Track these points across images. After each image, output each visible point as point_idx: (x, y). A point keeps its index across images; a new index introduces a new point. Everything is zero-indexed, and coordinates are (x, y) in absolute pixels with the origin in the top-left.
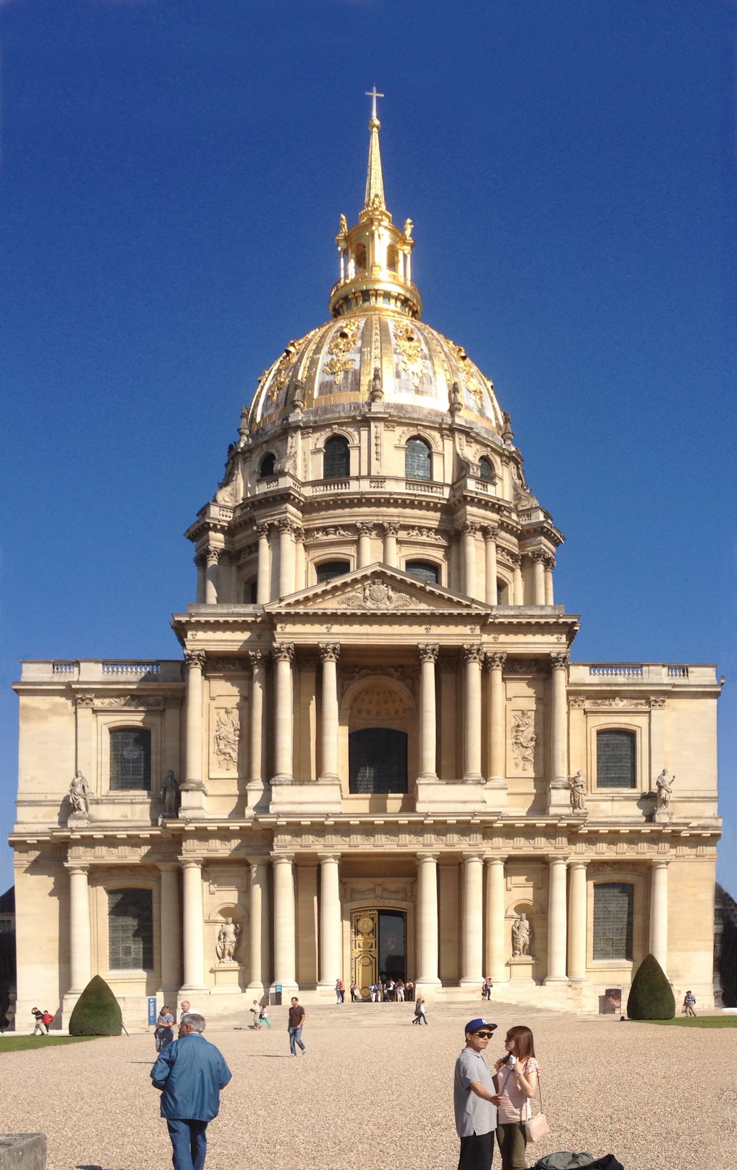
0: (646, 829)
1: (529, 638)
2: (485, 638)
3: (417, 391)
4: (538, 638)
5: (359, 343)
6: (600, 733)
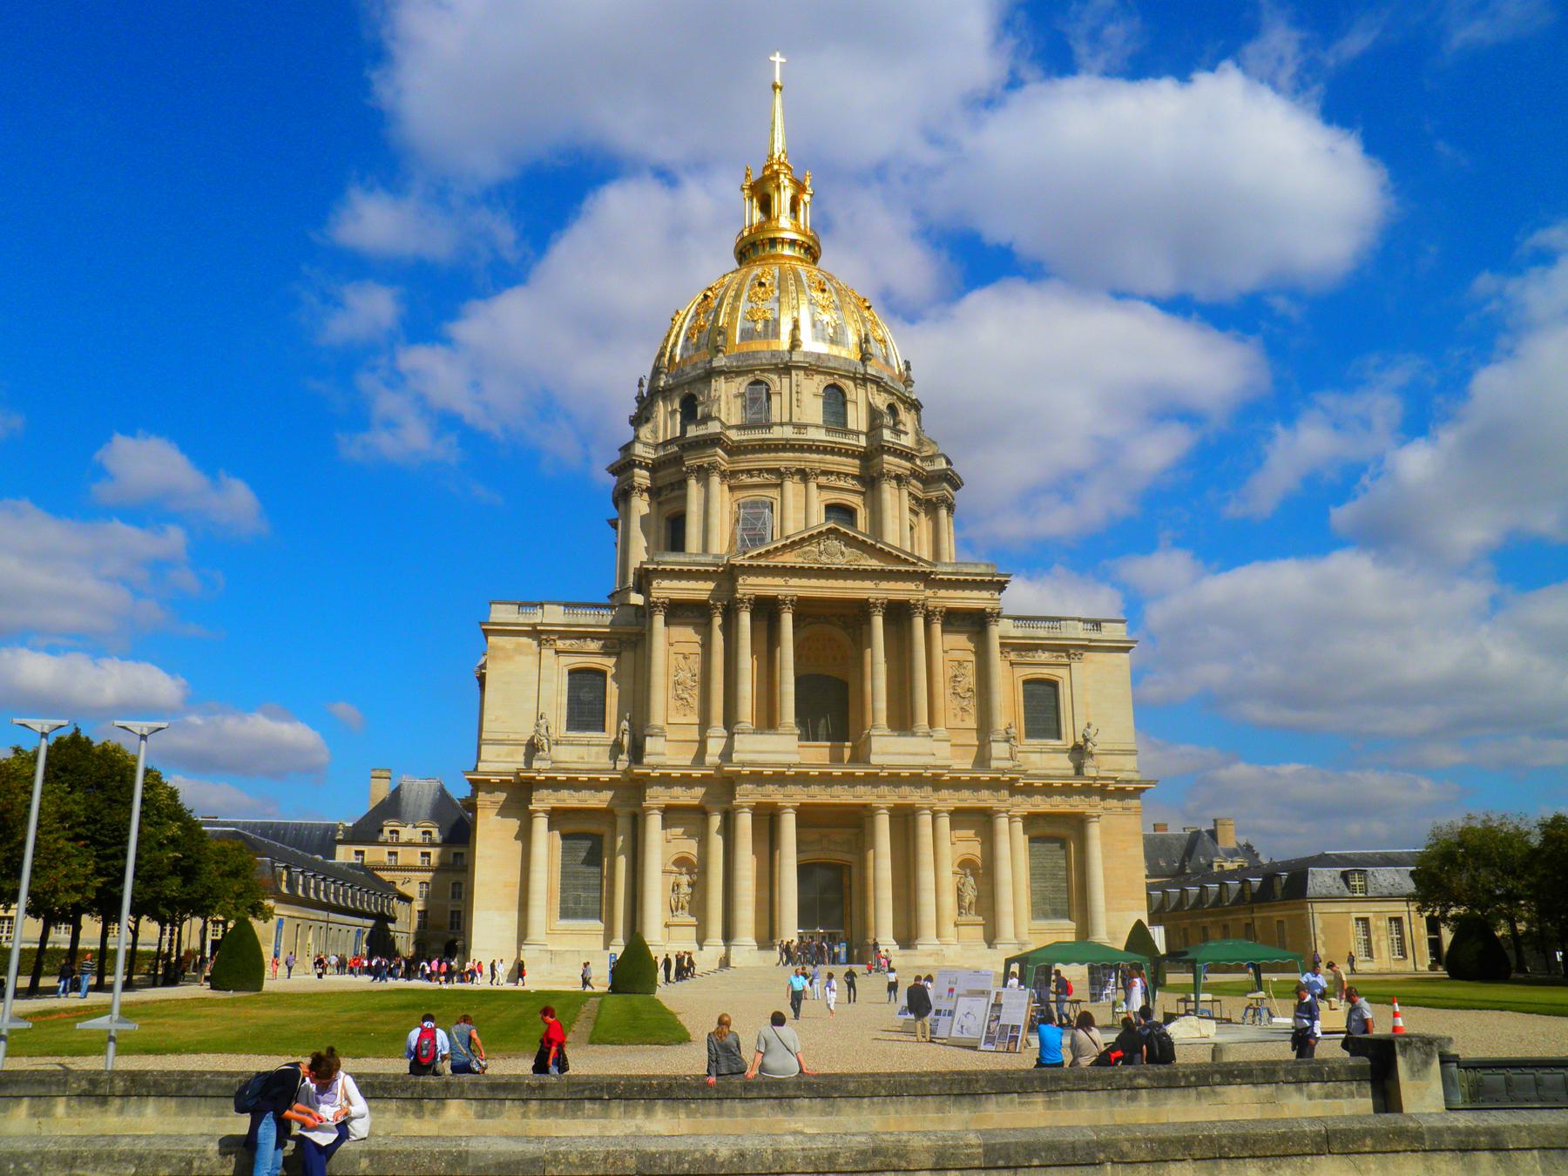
0: (1077, 783)
1: (967, 593)
2: (929, 593)
3: (833, 341)
4: (975, 594)
5: (777, 293)
6: (1026, 682)
